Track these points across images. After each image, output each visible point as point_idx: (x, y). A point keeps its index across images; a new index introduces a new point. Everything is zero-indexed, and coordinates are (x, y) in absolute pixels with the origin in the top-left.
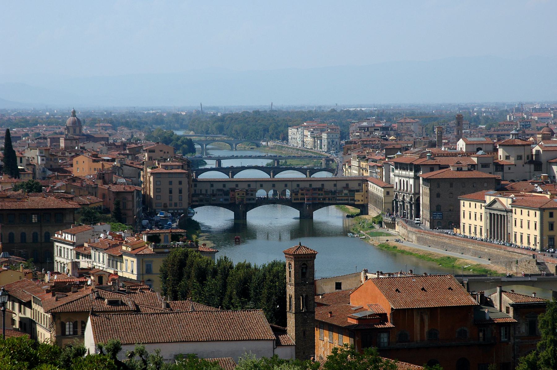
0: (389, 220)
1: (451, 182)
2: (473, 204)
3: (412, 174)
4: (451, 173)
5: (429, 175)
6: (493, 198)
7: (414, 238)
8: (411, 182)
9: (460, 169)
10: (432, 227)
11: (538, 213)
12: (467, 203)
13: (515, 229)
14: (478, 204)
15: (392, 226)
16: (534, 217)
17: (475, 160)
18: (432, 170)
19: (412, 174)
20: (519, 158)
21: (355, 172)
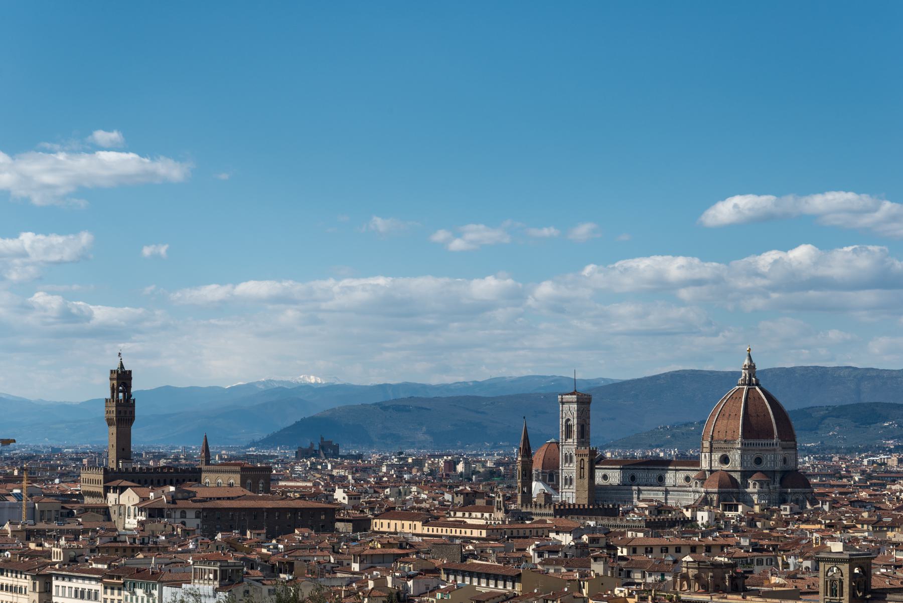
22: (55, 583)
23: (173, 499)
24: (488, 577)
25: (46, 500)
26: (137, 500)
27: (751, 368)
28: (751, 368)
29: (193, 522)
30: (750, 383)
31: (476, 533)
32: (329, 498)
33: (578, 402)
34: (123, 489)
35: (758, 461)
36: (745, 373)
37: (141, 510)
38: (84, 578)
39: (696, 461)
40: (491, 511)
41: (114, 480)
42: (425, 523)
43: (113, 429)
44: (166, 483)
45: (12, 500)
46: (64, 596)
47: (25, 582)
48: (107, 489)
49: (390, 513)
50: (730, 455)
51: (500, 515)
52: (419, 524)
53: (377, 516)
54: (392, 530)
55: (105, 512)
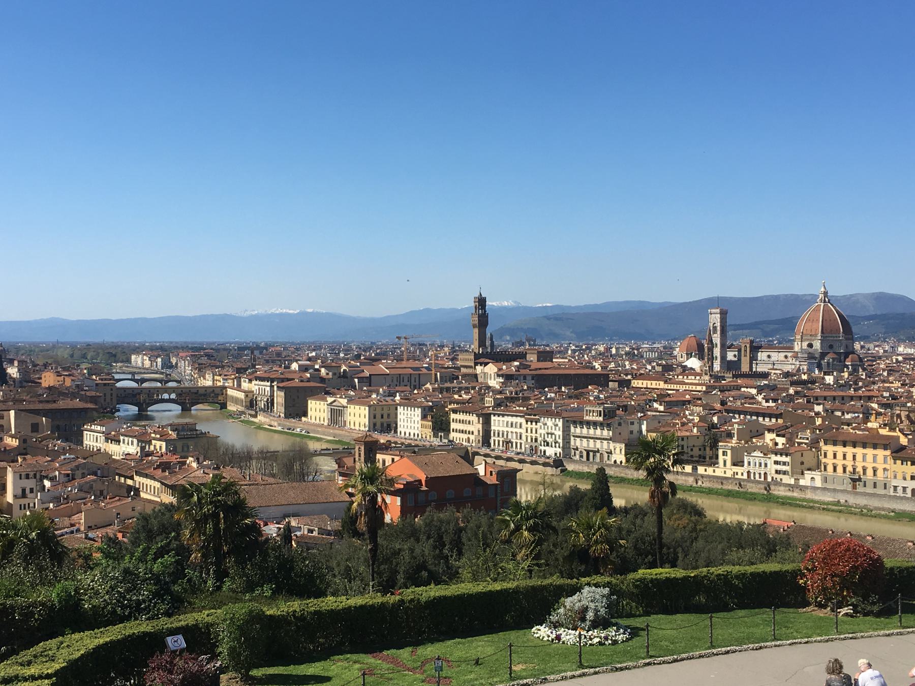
0: (253, 413)
1: (298, 389)
2: (318, 402)
3: (269, 384)
4: (296, 383)
5: (281, 385)
6: (333, 399)
7: (276, 424)
8: (268, 389)
9: (302, 381)
10: (286, 417)
11: (367, 408)
12: (313, 402)
13: (349, 418)
14: (322, 403)
15: (255, 416)
16: (364, 411)
17: (308, 375)
18: (283, 381)
19: (269, 384)
20: (334, 374)
21: (209, 383)
22: (493, 418)
23: (518, 368)
24: (770, 416)
25: (443, 370)
26: (496, 370)
27: (826, 294)
28: (826, 294)
29: (531, 383)
30: (825, 301)
31: (699, 388)
32: (593, 368)
33: (721, 313)
34: (486, 364)
35: (831, 347)
36: (821, 296)
37: (499, 376)
38: (512, 416)
39: (792, 348)
40: (700, 375)
41: (480, 359)
42: (666, 382)
43: (476, 330)
44: (515, 360)
45: (425, 371)
46: (499, 426)
47: (474, 418)
48: (476, 364)
49: (641, 377)
50: (814, 343)
51: (707, 378)
52: (662, 383)
53: (634, 379)
54: (645, 386)
55: (476, 376)
